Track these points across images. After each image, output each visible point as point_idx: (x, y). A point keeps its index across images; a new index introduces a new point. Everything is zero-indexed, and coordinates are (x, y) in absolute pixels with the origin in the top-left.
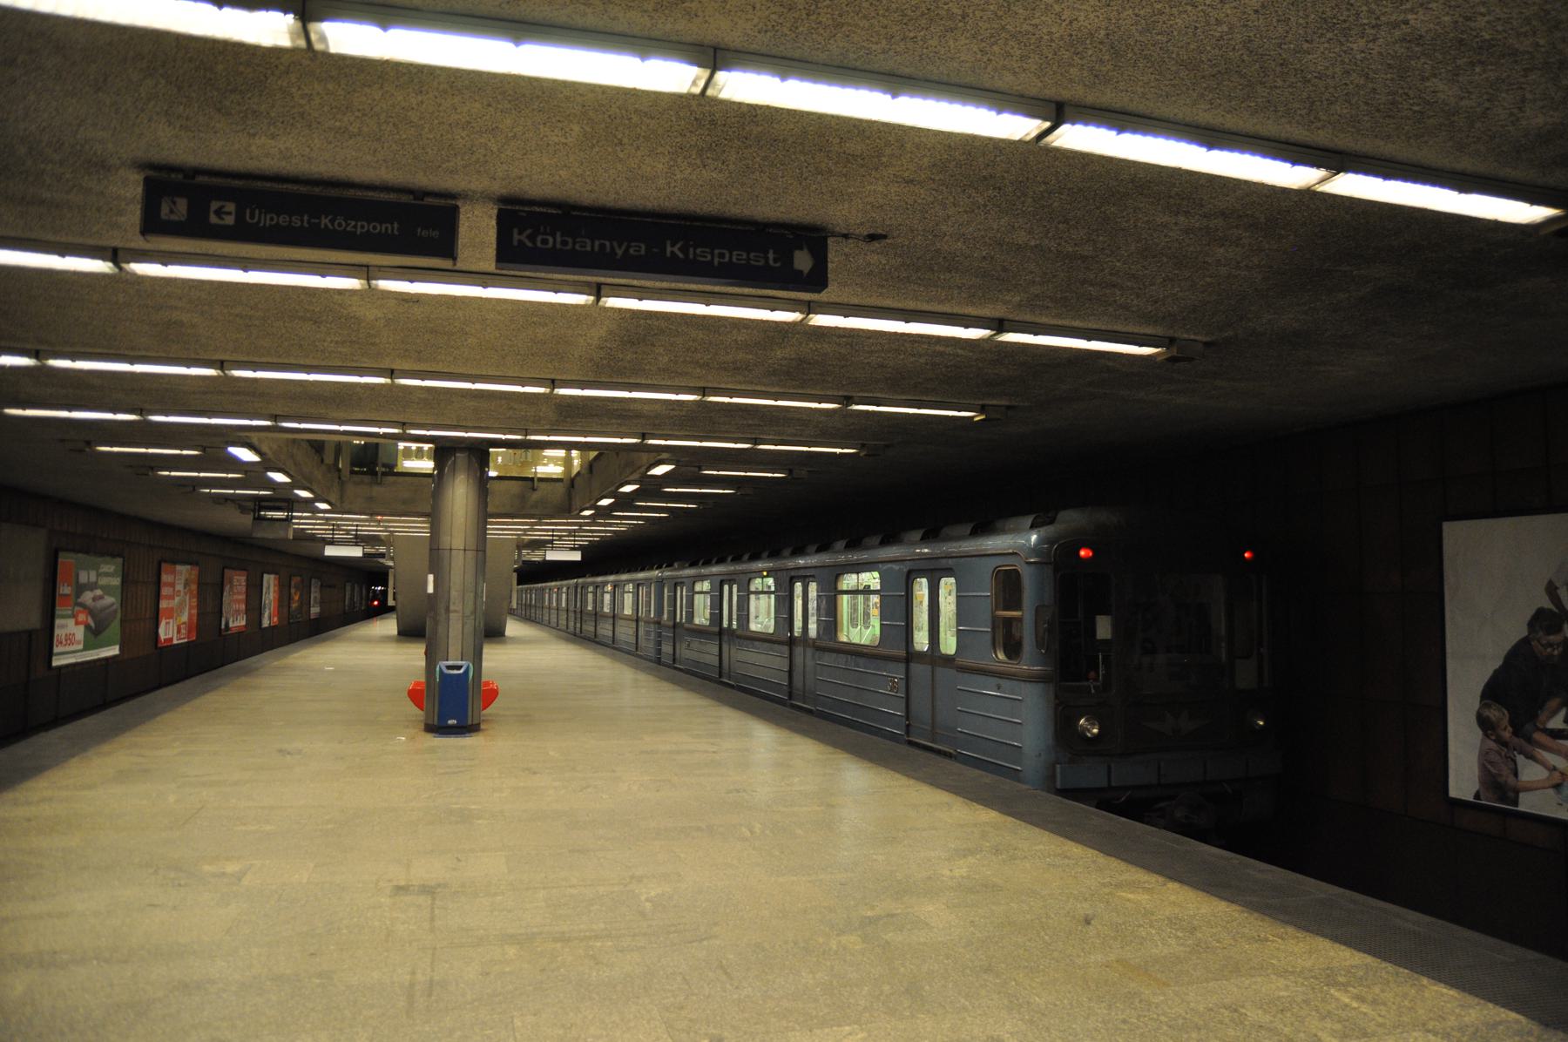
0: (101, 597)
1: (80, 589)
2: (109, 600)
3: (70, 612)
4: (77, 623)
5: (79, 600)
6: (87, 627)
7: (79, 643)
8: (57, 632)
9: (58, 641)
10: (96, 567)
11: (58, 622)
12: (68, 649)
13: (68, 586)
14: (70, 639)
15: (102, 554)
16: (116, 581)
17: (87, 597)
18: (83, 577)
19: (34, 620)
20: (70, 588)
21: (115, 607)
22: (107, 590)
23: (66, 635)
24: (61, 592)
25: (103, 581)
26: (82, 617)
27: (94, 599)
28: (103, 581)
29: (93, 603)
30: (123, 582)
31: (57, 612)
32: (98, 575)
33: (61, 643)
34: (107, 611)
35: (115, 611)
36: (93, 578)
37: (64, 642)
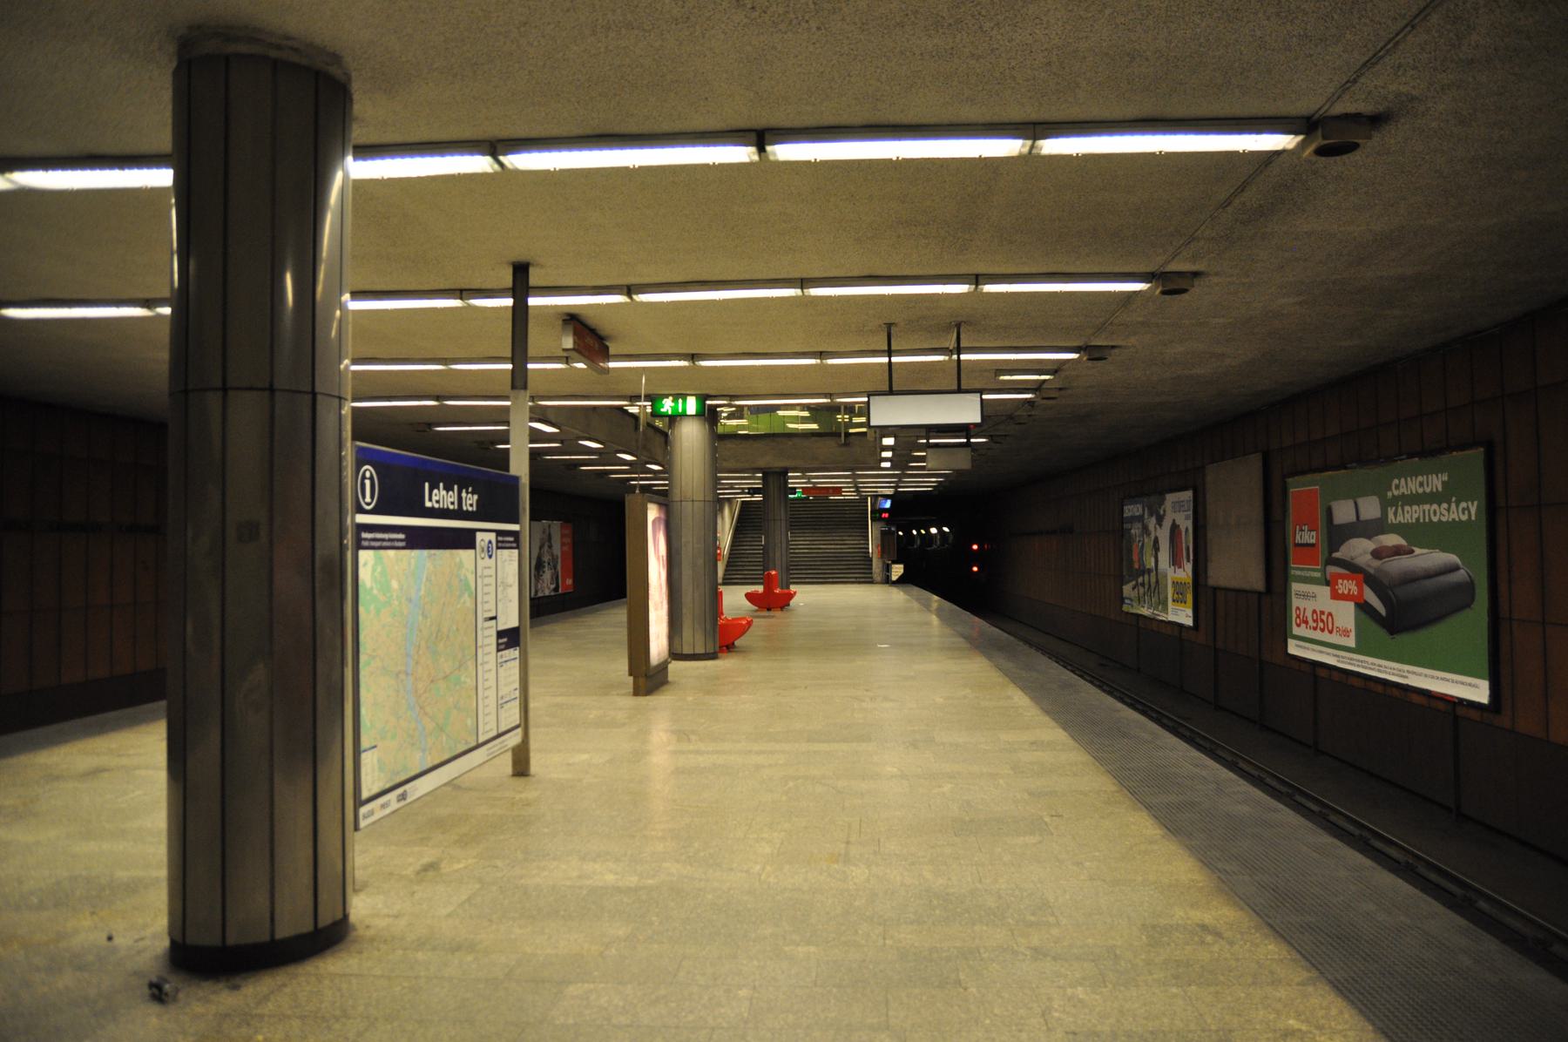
0: (1397, 551)
1: (1337, 535)
2: (1428, 558)
3: (1317, 575)
4: (1336, 596)
5: (1336, 555)
6: (1363, 607)
7: (1346, 633)
8: (1296, 602)
9: (1298, 616)
10: (1380, 490)
11: (1296, 587)
12: (1325, 637)
13: (1310, 530)
14: (1323, 620)
15: (1390, 459)
16: (1466, 511)
17: (1359, 549)
18: (1344, 513)
19: (1254, 579)
20: (1314, 533)
21: (1461, 575)
22: (1420, 534)
23: (1314, 612)
24: (1298, 540)
25: (1410, 514)
26: (1347, 586)
27: (1377, 554)
28: (1410, 514)
29: (1376, 563)
30: (1492, 510)
31: (1295, 570)
32: (1385, 504)
33: (1306, 622)
34: (1430, 584)
35: (1468, 588)
36: (1370, 508)
37: (1312, 624)
